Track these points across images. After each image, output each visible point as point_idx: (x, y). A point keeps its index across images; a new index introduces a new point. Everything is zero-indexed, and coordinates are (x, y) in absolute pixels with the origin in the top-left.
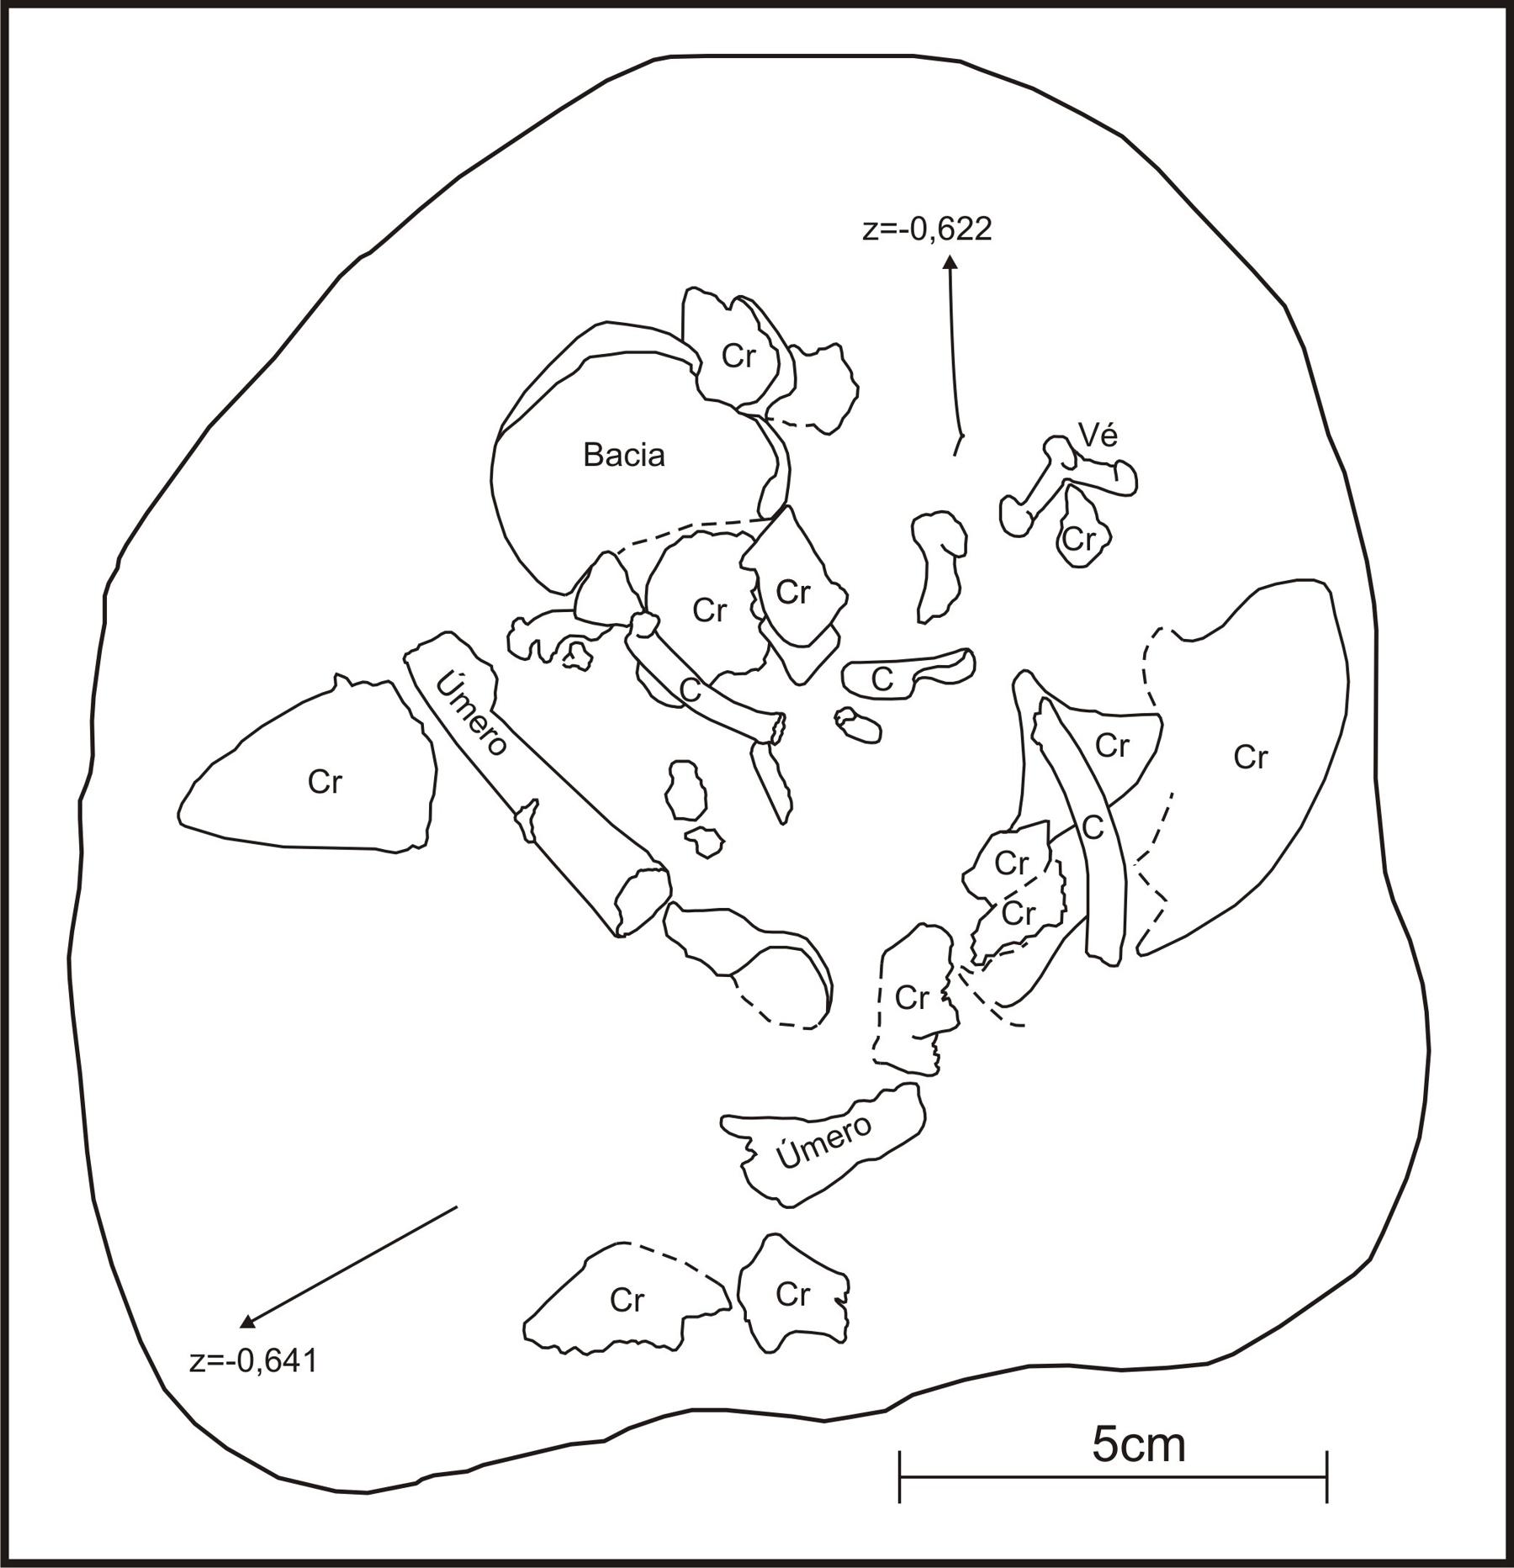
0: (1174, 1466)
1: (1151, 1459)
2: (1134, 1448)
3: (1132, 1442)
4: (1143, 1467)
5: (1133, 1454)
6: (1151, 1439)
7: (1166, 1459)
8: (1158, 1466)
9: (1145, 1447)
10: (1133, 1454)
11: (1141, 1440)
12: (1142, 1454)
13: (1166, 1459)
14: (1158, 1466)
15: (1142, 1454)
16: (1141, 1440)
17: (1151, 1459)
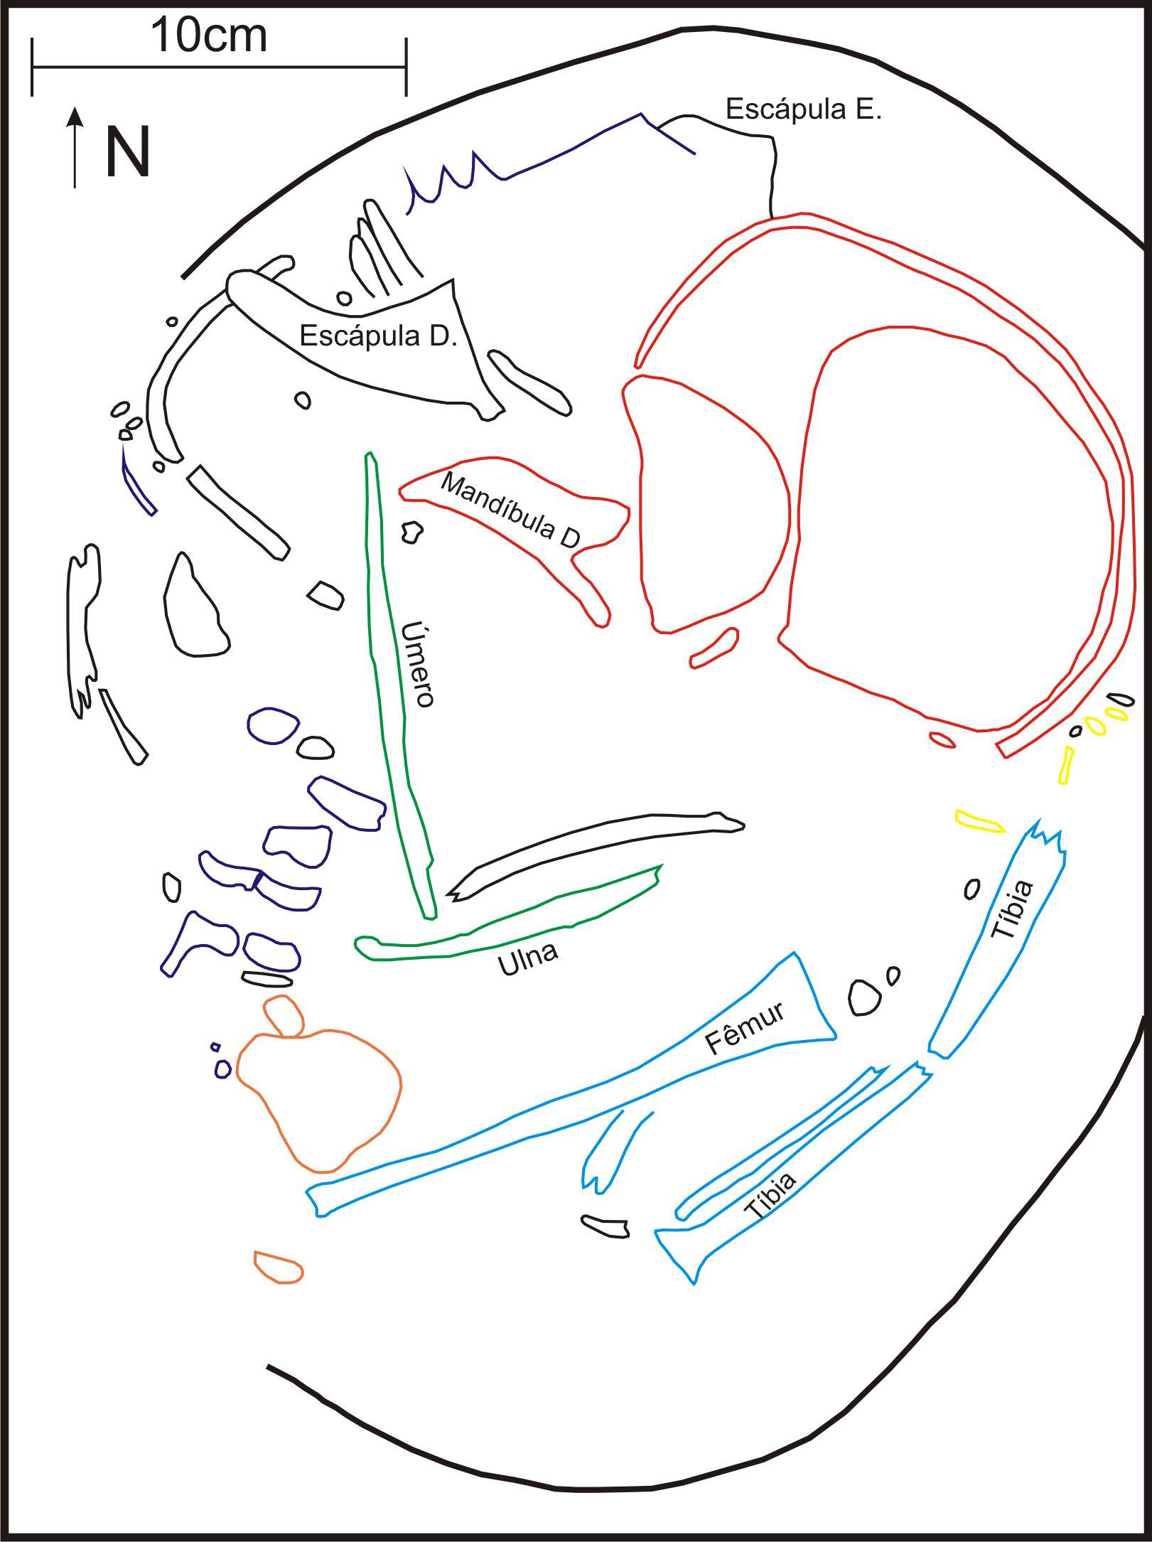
0: (255, 56)
1: (233, 49)
2: (217, 38)
3: (215, 34)
4: (226, 57)
5: (215, 43)
6: (234, 30)
7: (248, 49)
8: (240, 56)
9: (227, 37)
10: (215, 43)
11: (224, 31)
12: (224, 44)
13: (248, 49)
14: (240, 56)
15: (224, 44)
16: (224, 31)
17: (233, 49)
